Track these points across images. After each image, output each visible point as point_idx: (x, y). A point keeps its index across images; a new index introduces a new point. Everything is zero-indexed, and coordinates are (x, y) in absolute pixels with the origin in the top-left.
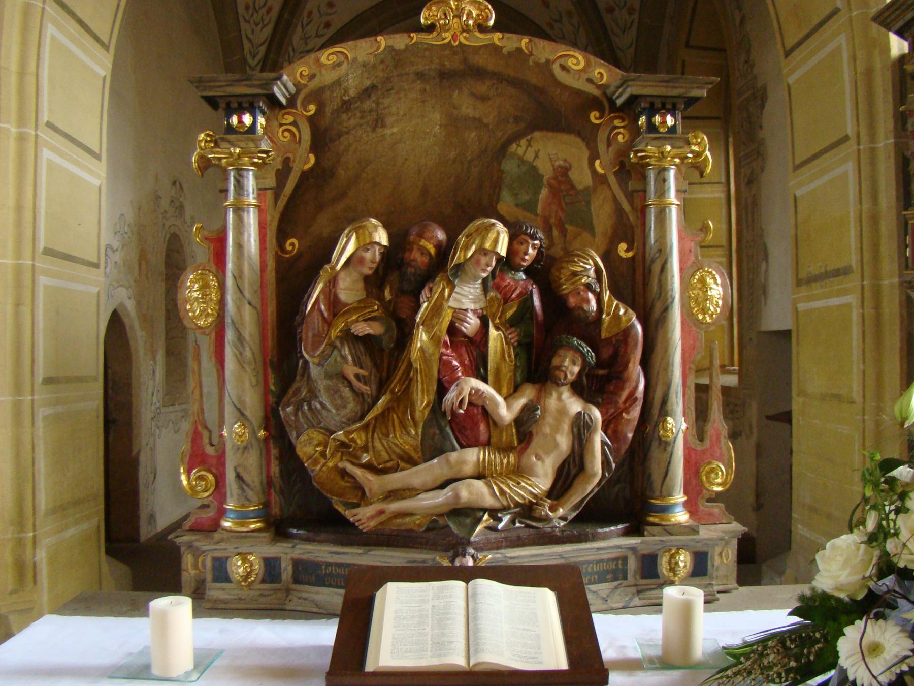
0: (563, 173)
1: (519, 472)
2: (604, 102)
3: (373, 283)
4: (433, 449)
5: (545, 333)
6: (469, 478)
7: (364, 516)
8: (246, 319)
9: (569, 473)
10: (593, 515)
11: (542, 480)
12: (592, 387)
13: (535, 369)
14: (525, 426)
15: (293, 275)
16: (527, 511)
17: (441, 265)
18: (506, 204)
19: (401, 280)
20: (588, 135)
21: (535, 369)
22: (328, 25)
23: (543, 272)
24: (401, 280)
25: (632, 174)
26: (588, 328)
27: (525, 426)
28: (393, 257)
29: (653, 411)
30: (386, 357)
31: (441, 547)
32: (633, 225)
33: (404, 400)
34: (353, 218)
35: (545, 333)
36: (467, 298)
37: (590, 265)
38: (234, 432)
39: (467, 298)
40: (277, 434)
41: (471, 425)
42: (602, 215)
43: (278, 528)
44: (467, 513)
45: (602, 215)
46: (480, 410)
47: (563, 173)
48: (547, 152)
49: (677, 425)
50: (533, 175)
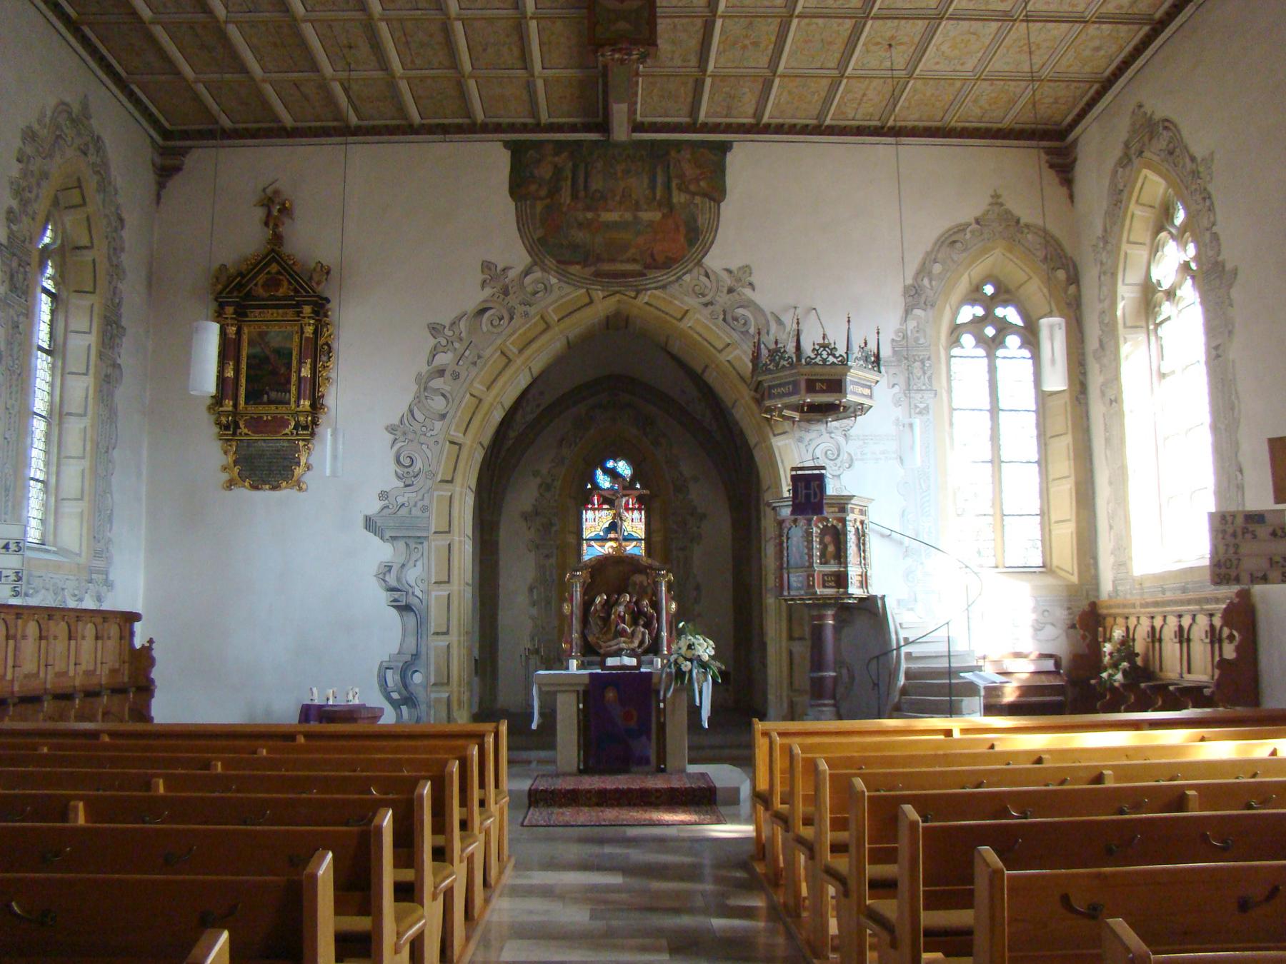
0: (641, 583)
1: (632, 642)
2: (650, 567)
3: (603, 606)
4: (615, 637)
5: (637, 615)
6: (623, 643)
7: (602, 651)
8: (577, 612)
9: (642, 643)
10: (646, 652)
11: (636, 644)
12: (645, 626)
13: (635, 623)
14: (633, 633)
15: (587, 604)
16: (633, 650)
17: (617, 603)
18: (630, 589)
19: (608, 606)
20: (647, 574)
21: (635, 623)
22: (538, 406)
23: (637, 603)
24: (608, 606)
25: (656, 585)
26: (645, 614)
27: (633, 633)
28: (607, 601)
29: (659, 630)
30: (606, 620)
31: (618, 653)
32: (656, 593)
33: (609, 629)
34: (599, 594)
35: (637, 615)
36: (621, 609)
37: (646, 602)
38: (575, 635)
39: (621, 609)
40: (584, 636)
41: (622, 633)
42: (650, 591)
43: (583, 655)
44: (622, 650)
45: (650, 591)
46: (624, 630)
47: (641, 583)
48: (639, 578)
49: (664, 634)
50: (635, 584)
